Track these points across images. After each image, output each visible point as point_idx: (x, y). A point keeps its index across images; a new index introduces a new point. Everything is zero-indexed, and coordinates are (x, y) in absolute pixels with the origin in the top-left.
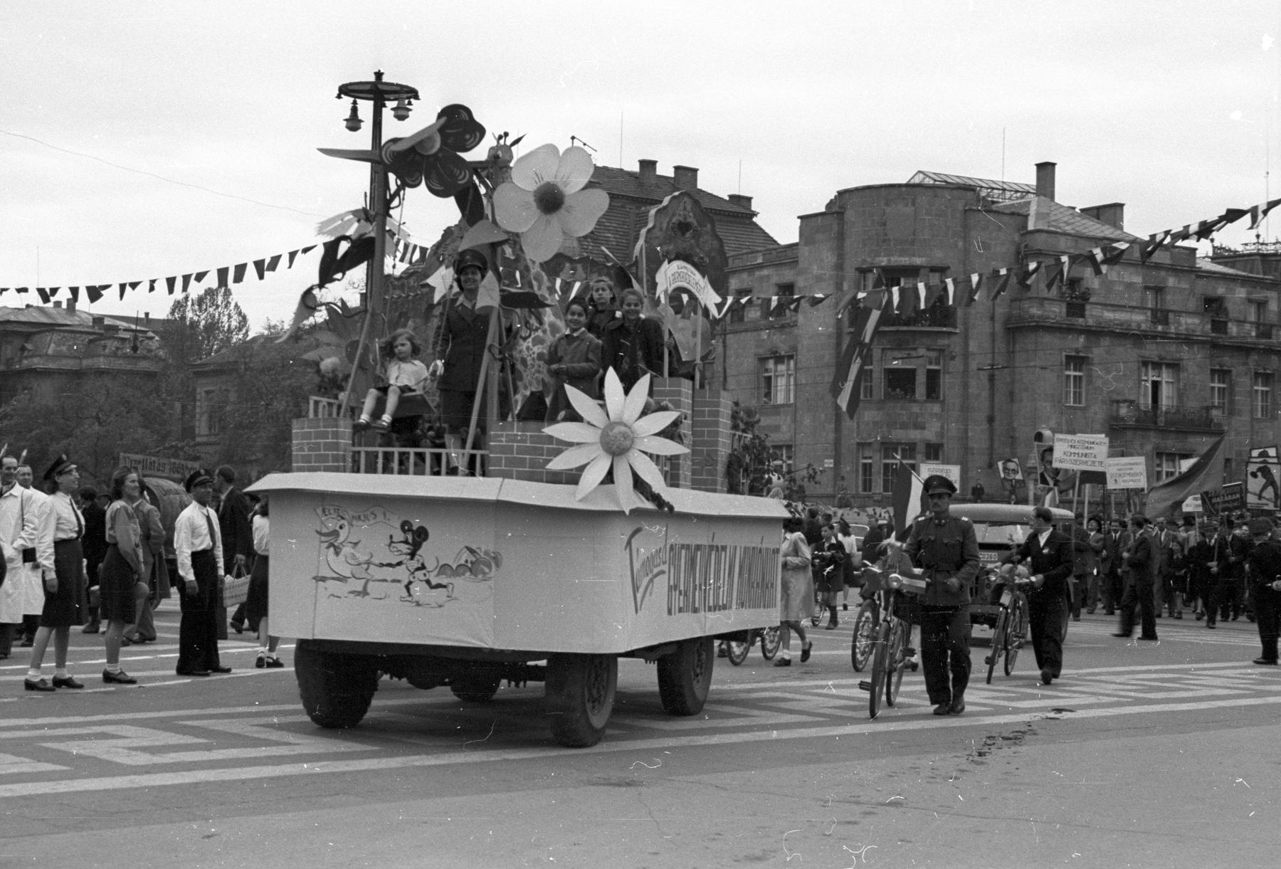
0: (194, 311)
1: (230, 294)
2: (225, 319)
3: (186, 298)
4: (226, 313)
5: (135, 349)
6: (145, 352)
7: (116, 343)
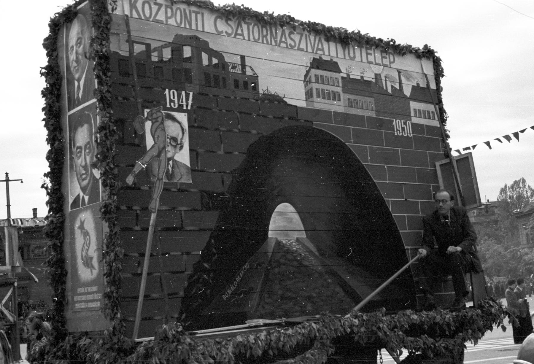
0: (510, 192)
1: (525, 182)
2: (525, 193)
3: (506, 186)
4: (525, 190)
5: (487, 212)
6: (492, 213)
7: (478, 211)
